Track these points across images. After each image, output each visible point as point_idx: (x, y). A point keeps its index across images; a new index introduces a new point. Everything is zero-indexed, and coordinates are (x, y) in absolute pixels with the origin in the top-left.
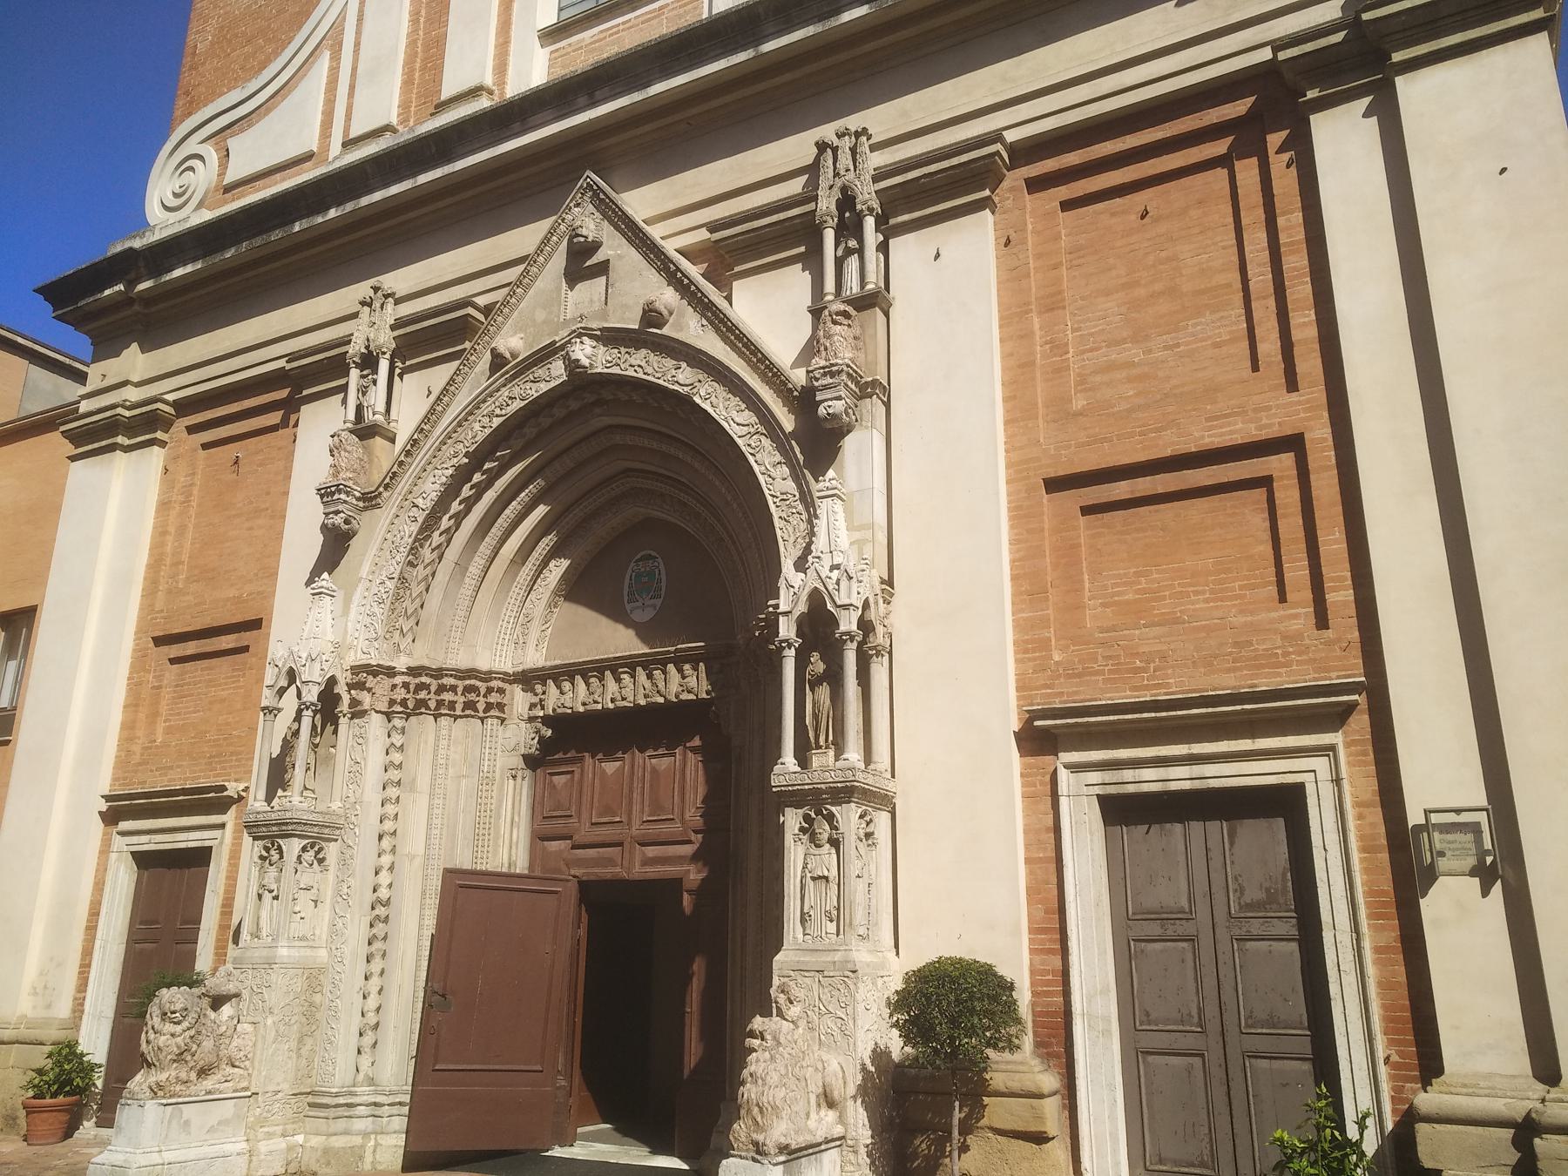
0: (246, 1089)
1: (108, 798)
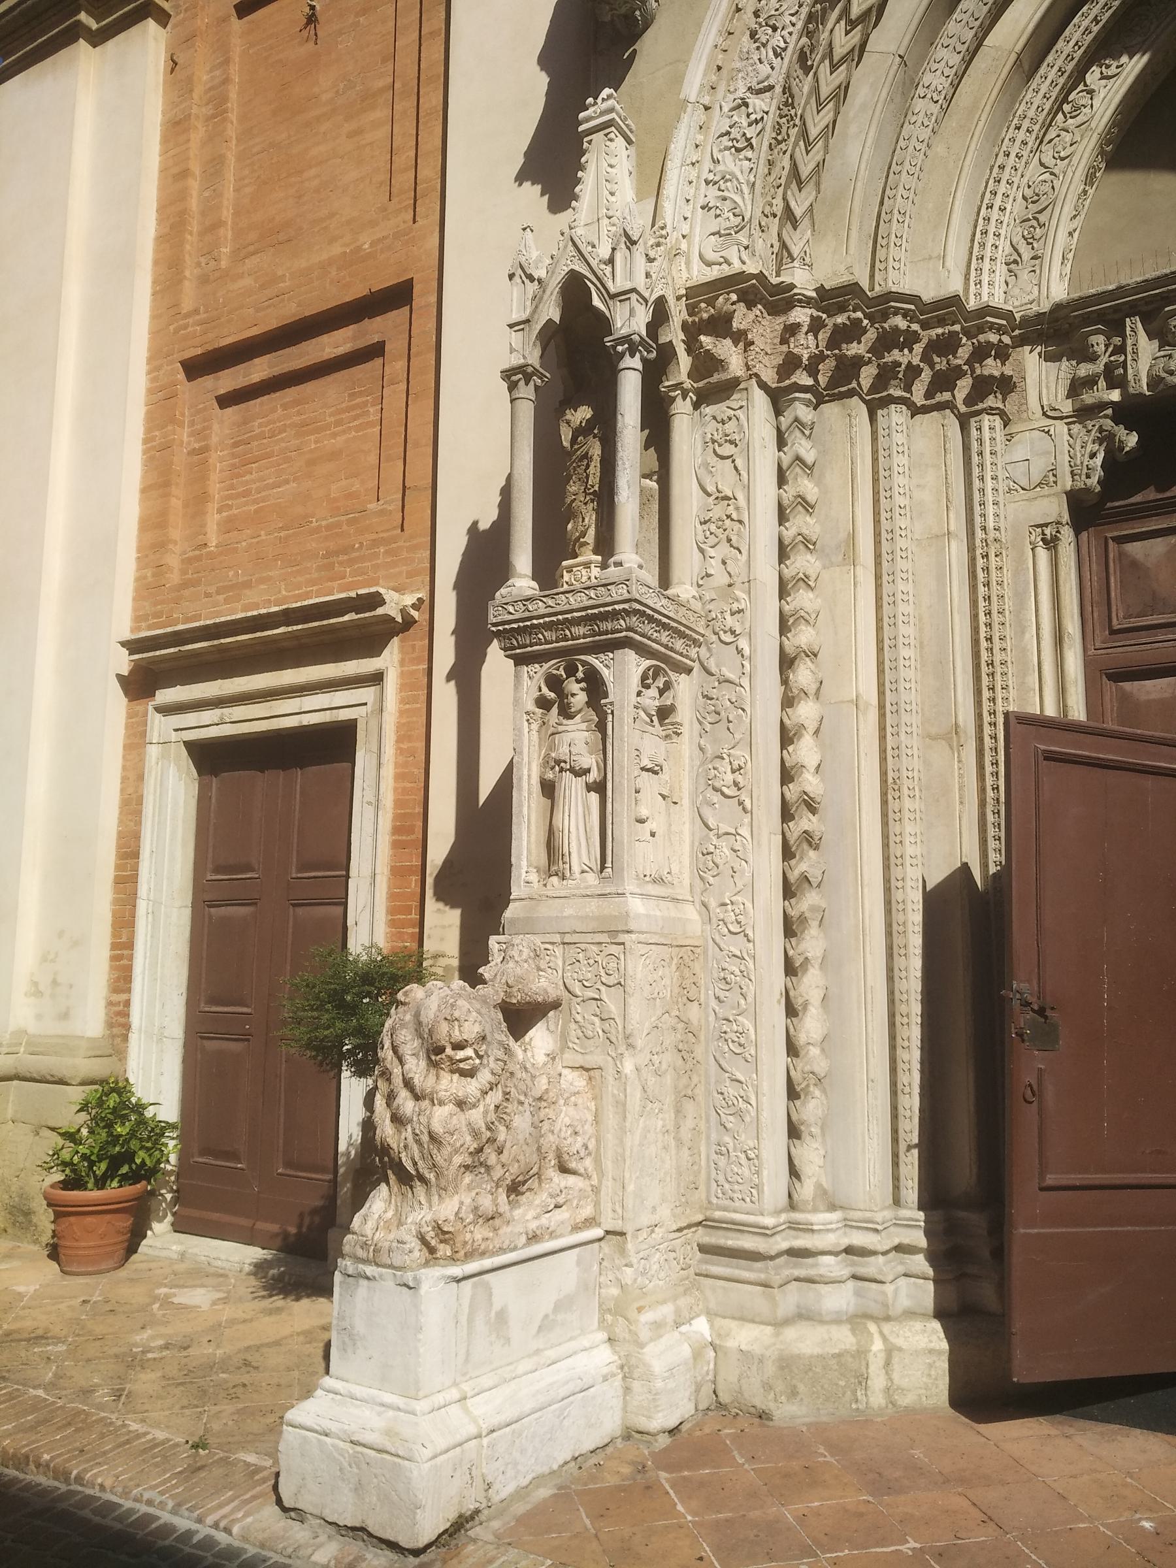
0: (590, 1222)
1: (133, 646)
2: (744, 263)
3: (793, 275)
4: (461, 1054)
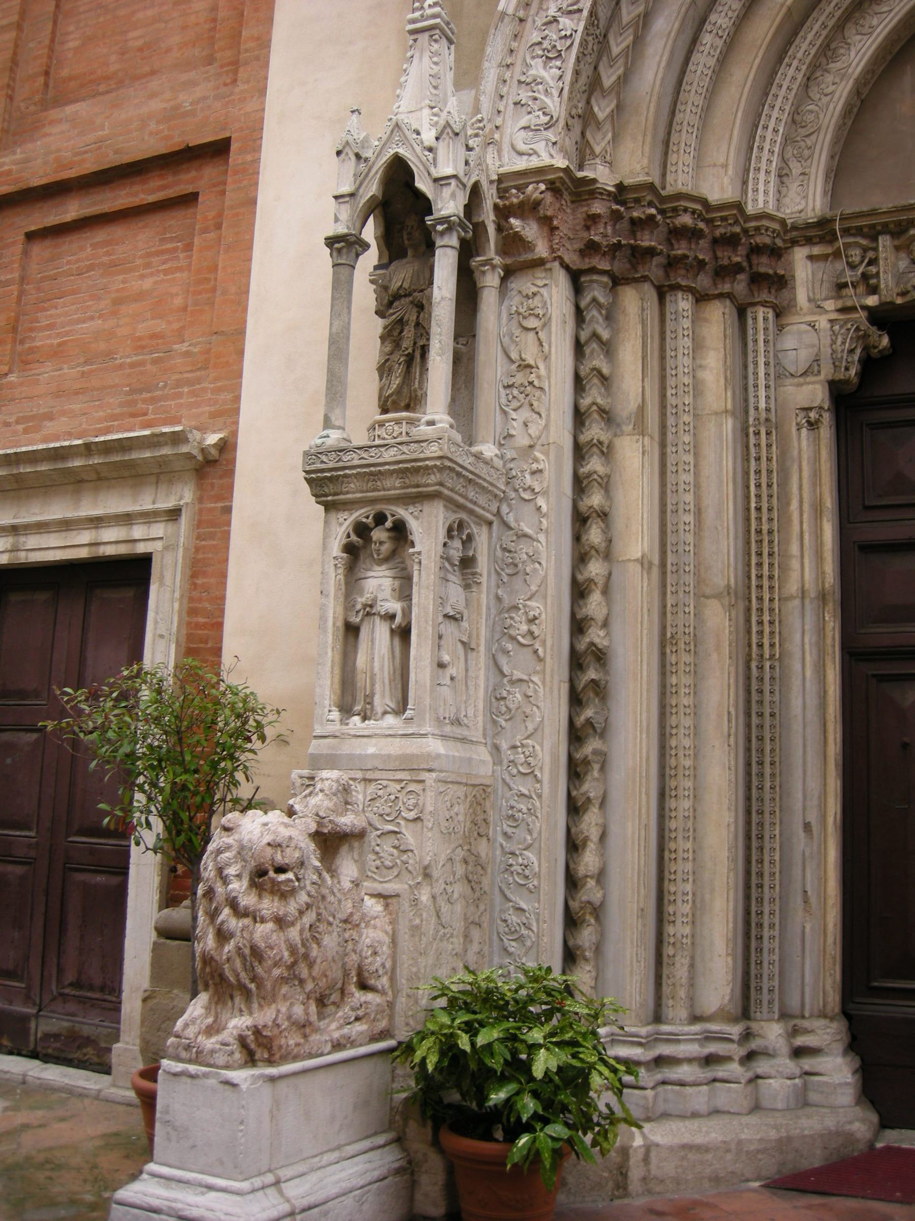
0: (384, 1035)
2: (552, 156)
3: (595, 170)
4: (282, 877)
